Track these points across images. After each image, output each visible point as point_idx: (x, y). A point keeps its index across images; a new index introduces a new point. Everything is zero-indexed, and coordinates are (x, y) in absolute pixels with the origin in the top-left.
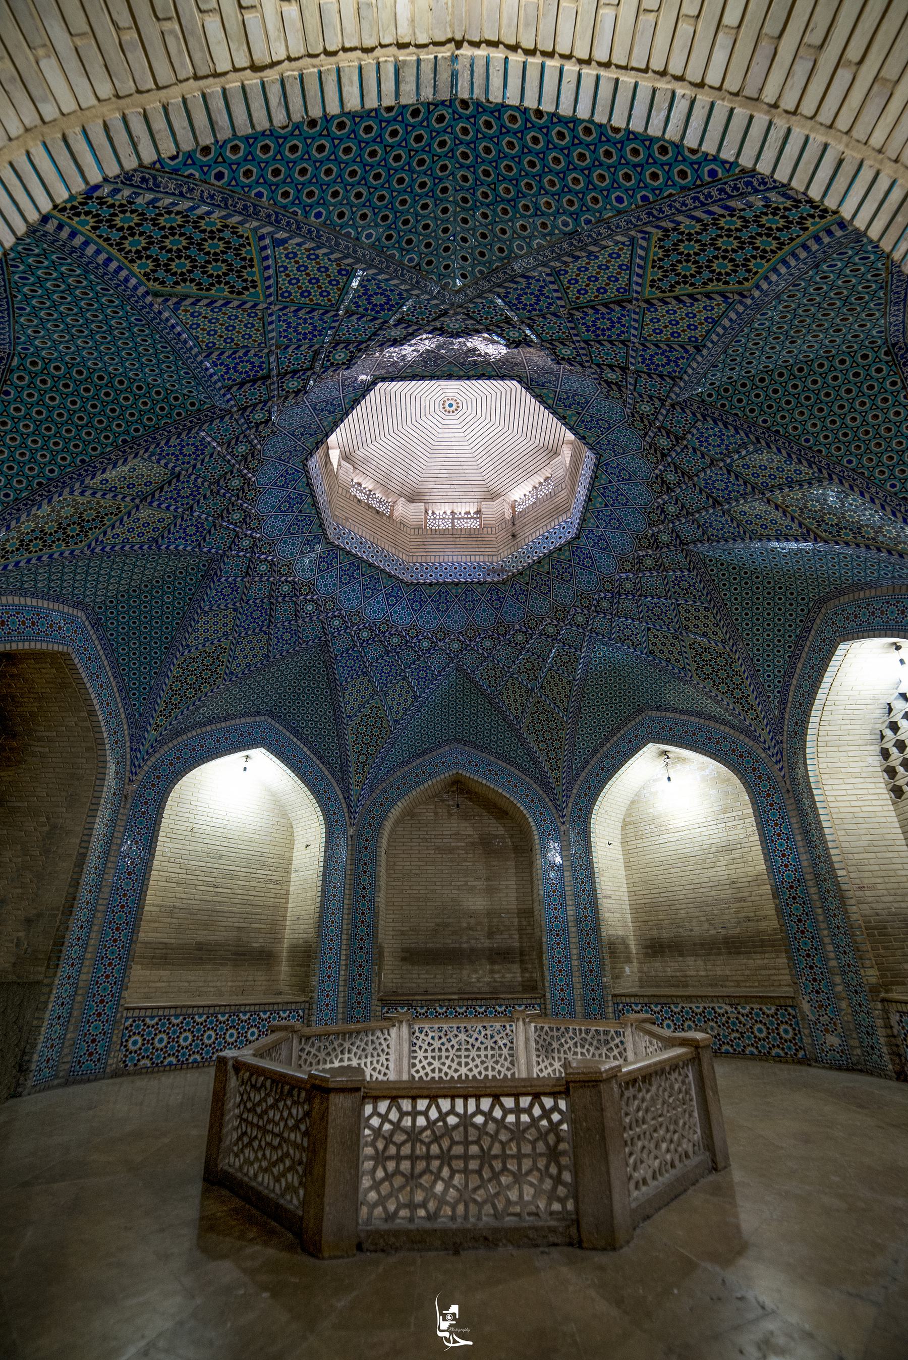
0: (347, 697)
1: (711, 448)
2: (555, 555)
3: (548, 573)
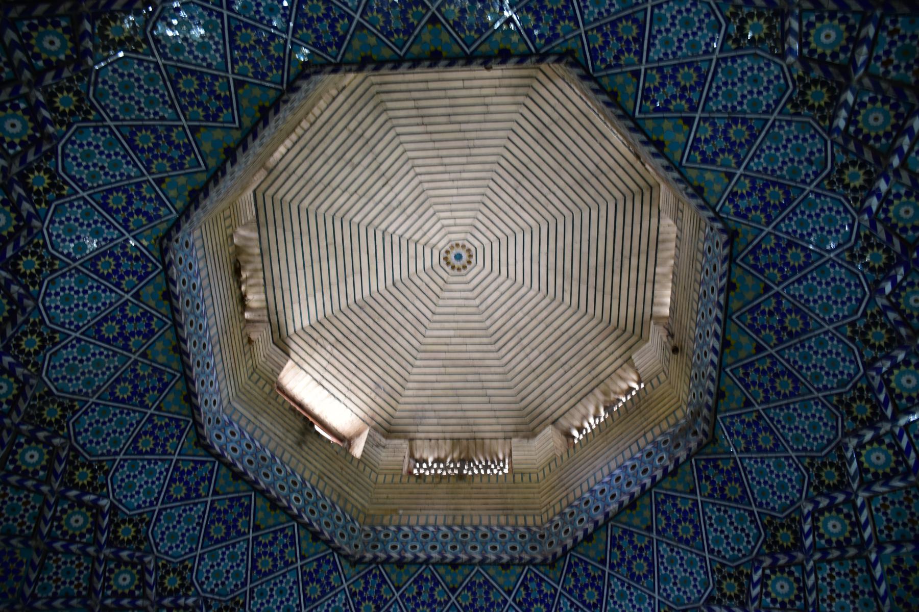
2: (735, 305)
3: (759, 349)
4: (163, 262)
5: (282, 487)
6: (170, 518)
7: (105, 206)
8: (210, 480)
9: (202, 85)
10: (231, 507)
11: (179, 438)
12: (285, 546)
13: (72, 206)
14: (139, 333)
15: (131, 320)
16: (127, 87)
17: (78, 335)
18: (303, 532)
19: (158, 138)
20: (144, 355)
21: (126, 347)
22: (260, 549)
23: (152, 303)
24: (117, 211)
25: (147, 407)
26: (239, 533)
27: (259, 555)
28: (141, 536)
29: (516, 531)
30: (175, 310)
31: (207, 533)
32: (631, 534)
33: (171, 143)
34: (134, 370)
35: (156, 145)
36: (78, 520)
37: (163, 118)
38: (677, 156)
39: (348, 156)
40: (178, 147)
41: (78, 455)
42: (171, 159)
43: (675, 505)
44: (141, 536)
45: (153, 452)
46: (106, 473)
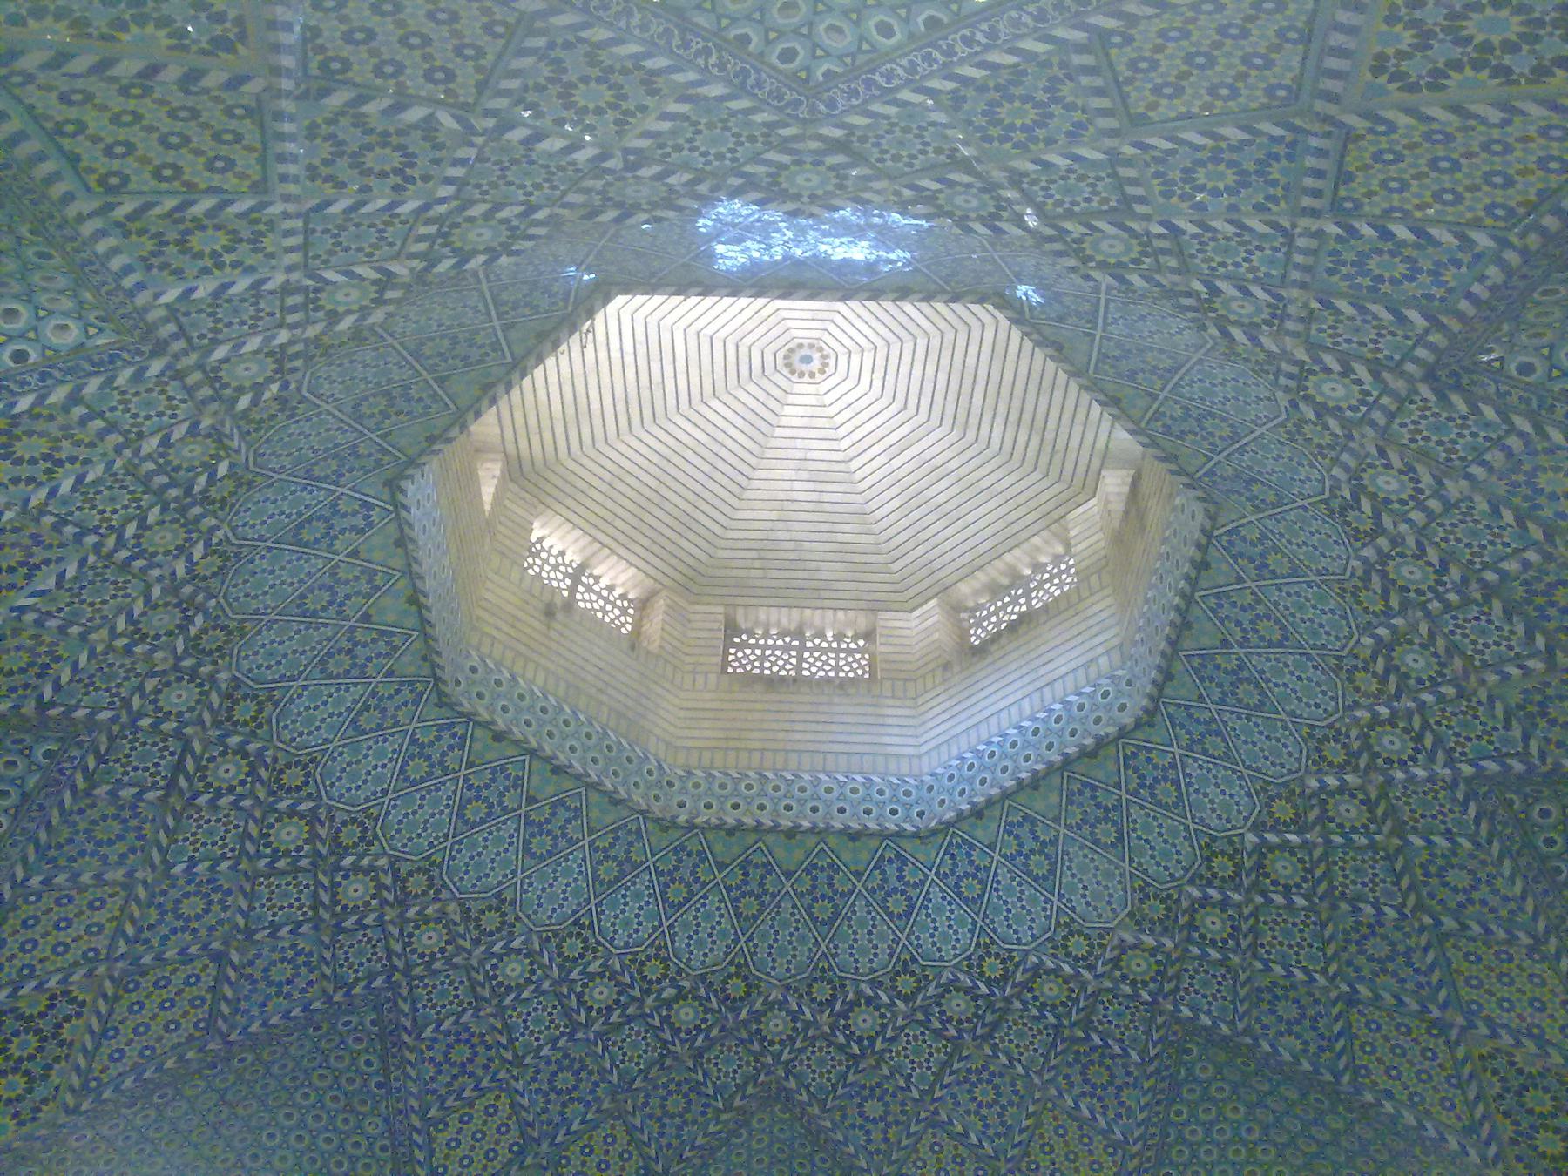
1: (276, 956)
7: (908, 914)
9: (743, 895)
15: (1021, 845)
20: (1056, 820)
21: (1054, 842)
22: (1254, 639)
25: (1119, 800)
30: (990, 802)
35: (823, 897)
37: (794, 906)
38: (402, 583)
39: (792, 556)
40: (815, 879)
42: (831, 878)
45: (1176, 783)
46: (1214, 839)
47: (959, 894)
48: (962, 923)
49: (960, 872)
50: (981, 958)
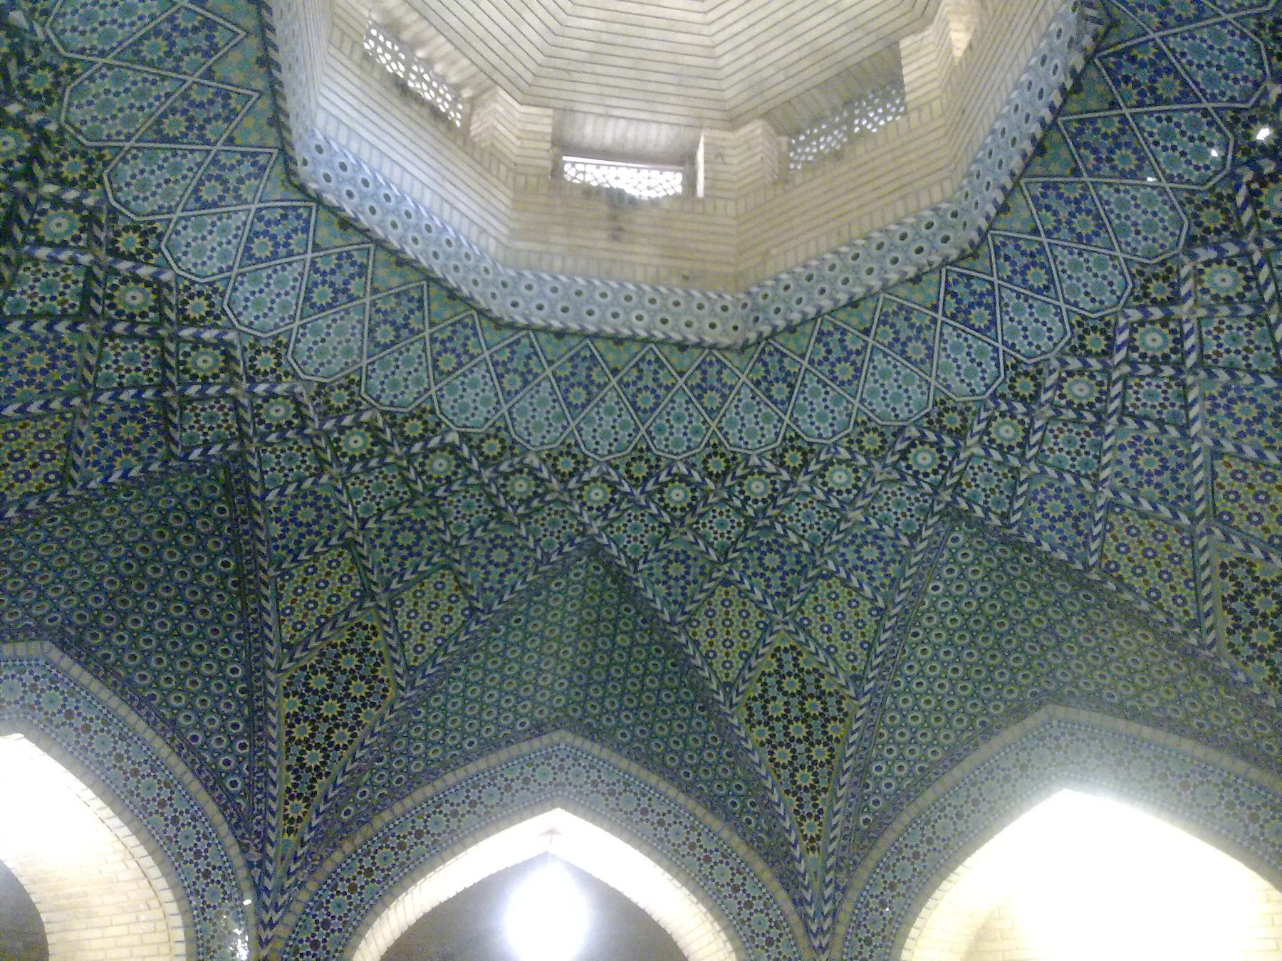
0: (1137, 583)
4: (310, 198)
5: (615, 315)
6: (523, 412)
8: (536, 354)
10: (575, 367)
11: (476, 335)
12: (656, 372)
13: (178, 233)
14: (352, 276)
15: (333, 272)
16: (106, 105)
17: (298, 322)
18: (666, 349)
19: (184, 112)
21: (352, 299)
22: (632, 389)
23: (339, 242)
24: (222, 198)
25: (420, 331)
26: (599, 386)
27: (635, 396)
28: (508, 443)
29: (919, 219)
30: (364, 231)
31: (569, 405)
32: (1056, 187)
33: (201, 105)
34: (378, 311)
36: (440, 465)
37: (168, 95)
41: (393, 416)
42: (217, 117)
43: (1097, 131)
44: (508, 443)
46: (432, 411)
47: (250, 240)
48: (224, 256)
49: (273, 230)
50: (200, 294)
